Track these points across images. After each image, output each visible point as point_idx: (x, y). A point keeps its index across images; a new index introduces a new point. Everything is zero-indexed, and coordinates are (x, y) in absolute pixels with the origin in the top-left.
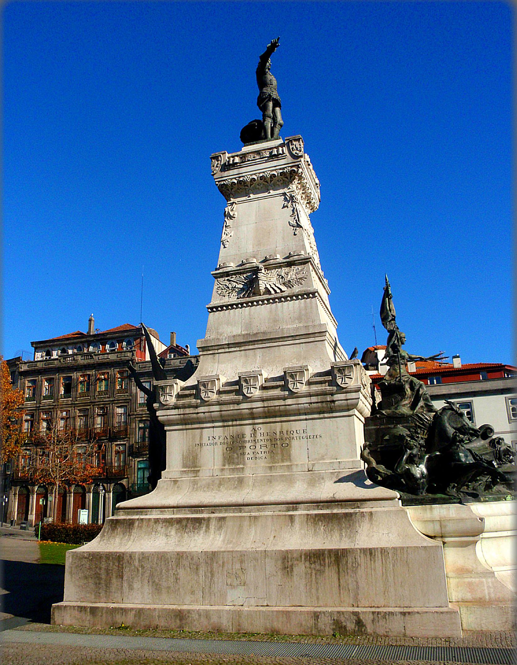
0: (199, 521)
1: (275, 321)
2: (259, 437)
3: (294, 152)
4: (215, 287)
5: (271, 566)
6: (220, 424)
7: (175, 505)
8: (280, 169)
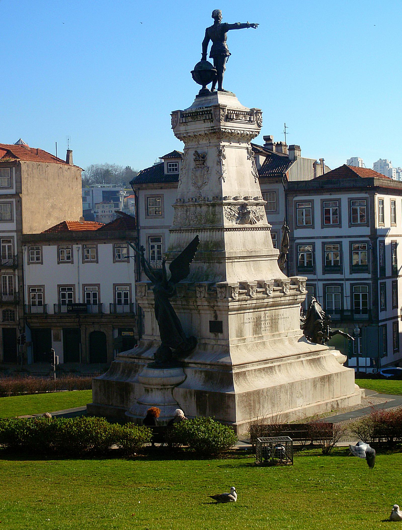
0: (271, 368)
1: (255, 243)
2: (267, 319)
3: (259, 122)
4: (224, 213)
5: (310, 385)
6: (252, 311)
7: (257, 361)
8: (251, 131)
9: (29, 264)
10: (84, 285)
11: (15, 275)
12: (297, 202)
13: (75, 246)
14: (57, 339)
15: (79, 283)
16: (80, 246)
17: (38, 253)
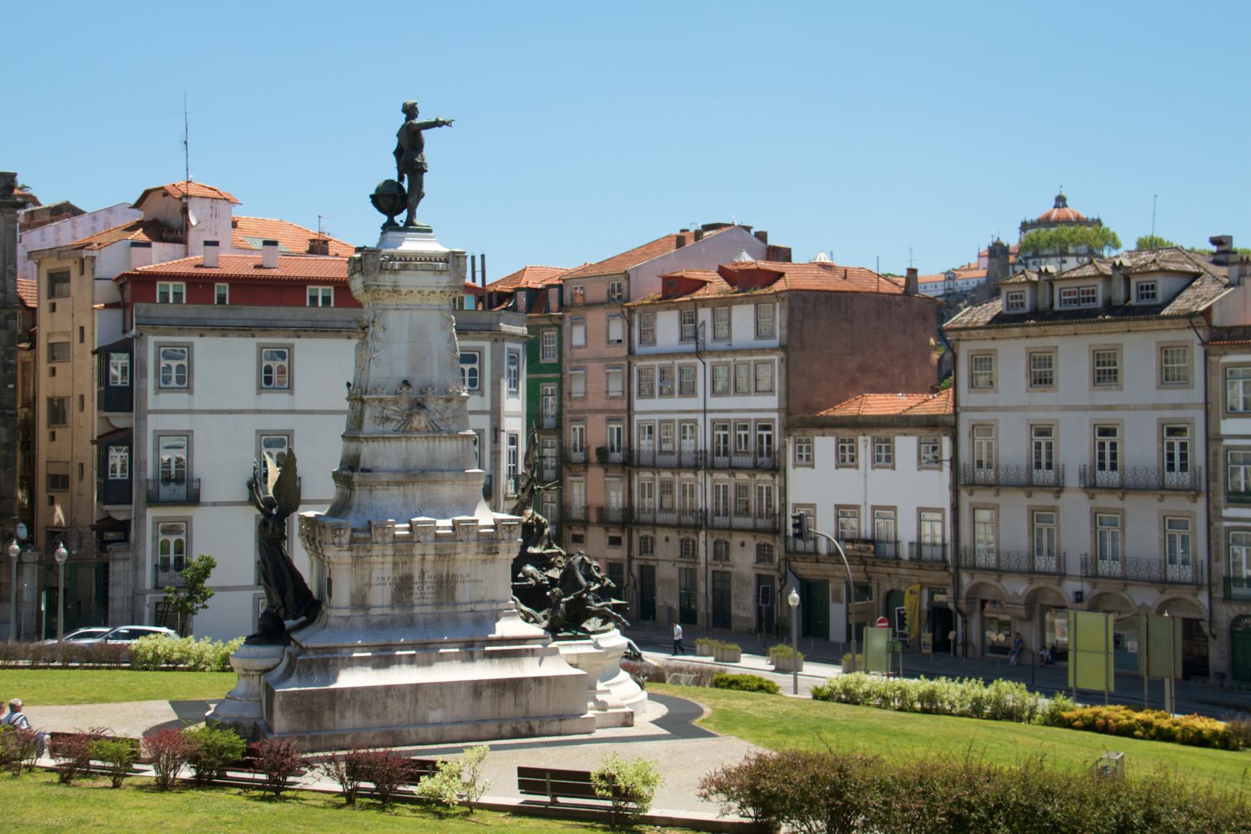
2: (426, 579)
9: (795, 466)
10: (874, 508)
11: (774, 485)
12: (1227, 366)
13: (861, 439)
14: (837, 599)
15: (865, 504)
16: (869, 438)
17: (888, 449)
